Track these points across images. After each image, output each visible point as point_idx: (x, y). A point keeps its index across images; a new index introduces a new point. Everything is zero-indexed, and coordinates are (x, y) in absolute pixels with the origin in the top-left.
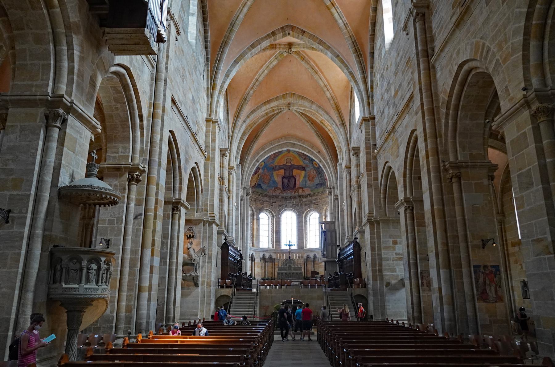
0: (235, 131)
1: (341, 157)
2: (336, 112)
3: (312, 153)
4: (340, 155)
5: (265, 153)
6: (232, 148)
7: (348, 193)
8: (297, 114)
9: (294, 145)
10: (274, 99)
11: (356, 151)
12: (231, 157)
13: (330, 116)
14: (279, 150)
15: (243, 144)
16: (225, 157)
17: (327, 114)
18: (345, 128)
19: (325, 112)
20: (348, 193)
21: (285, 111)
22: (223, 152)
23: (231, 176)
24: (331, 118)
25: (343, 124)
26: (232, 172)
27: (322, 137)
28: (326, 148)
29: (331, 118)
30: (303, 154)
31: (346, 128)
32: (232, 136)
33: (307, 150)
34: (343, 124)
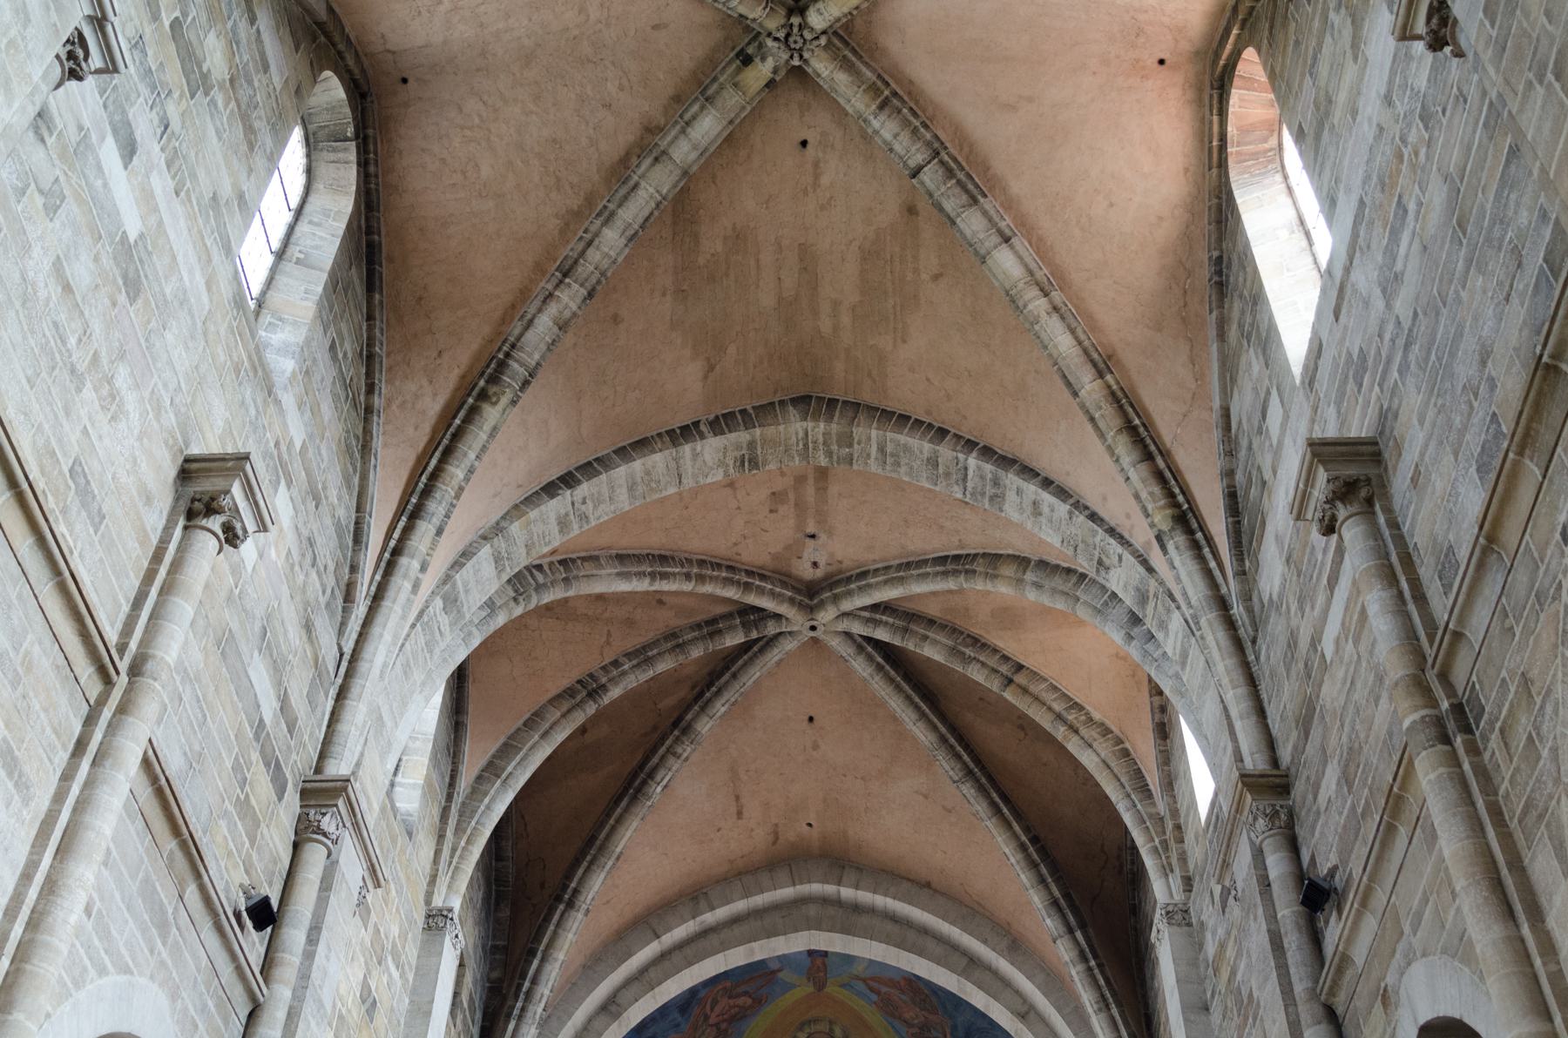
0: (403, 561)
1: (1176, 882)
2: (1126, 452)
3: (971, 966)
4: (1166, 870)
5: (667, 962)
6: (363, 666)
7: (1300, 987)
8: (860, 666)
9: (851, 917)
10: (703, 428)
11: (1351, 471)
12: (342, 727)
13: (1079, 506)
14: (761, 950)
15: (500, 808)
16: (215, 523)
17: (1062, 493)
18: (1195, 546)
19: (1047, 483)
20: (1300, 987)
21: (789, 645)
22: (205, 486)
23: (315, 855)
24: (1094, 517)
25: (1186, 519)
26: (328, 823)
27: (1027, 830)
28: (1055, 903)
29: (1094, 517)
30: (914, 984)
31: (1209, 540)
32: (377, 598)
33: (931, 944)
34: (1186, 519)
